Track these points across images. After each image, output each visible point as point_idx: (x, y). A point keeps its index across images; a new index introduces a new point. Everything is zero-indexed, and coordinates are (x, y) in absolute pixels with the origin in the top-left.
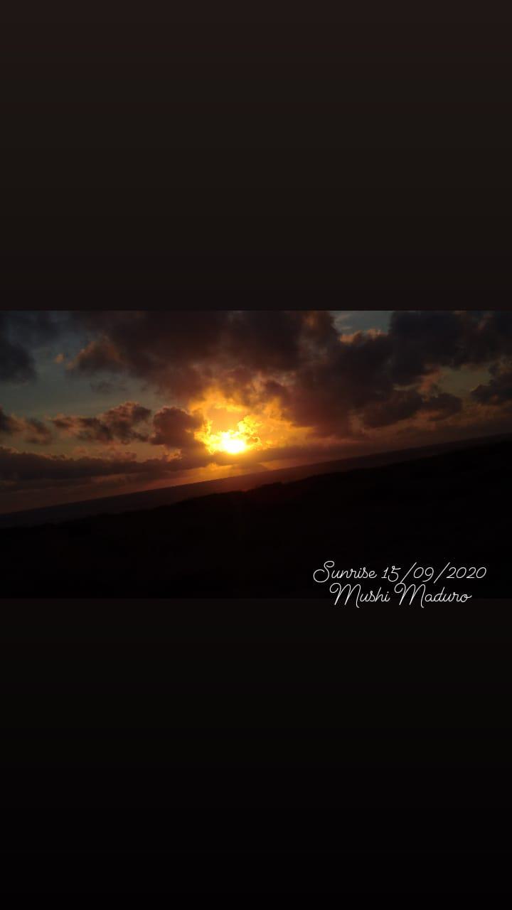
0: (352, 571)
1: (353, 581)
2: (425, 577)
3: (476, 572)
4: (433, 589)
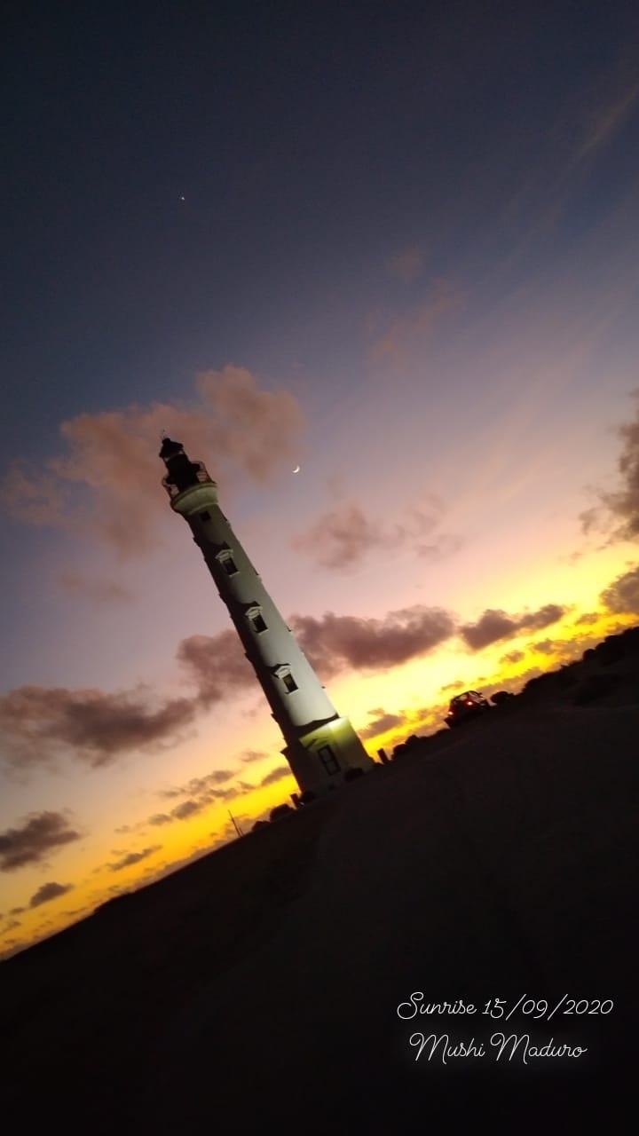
0: (445, 1004)
2: (536, 1013)
3: (600, 1006)
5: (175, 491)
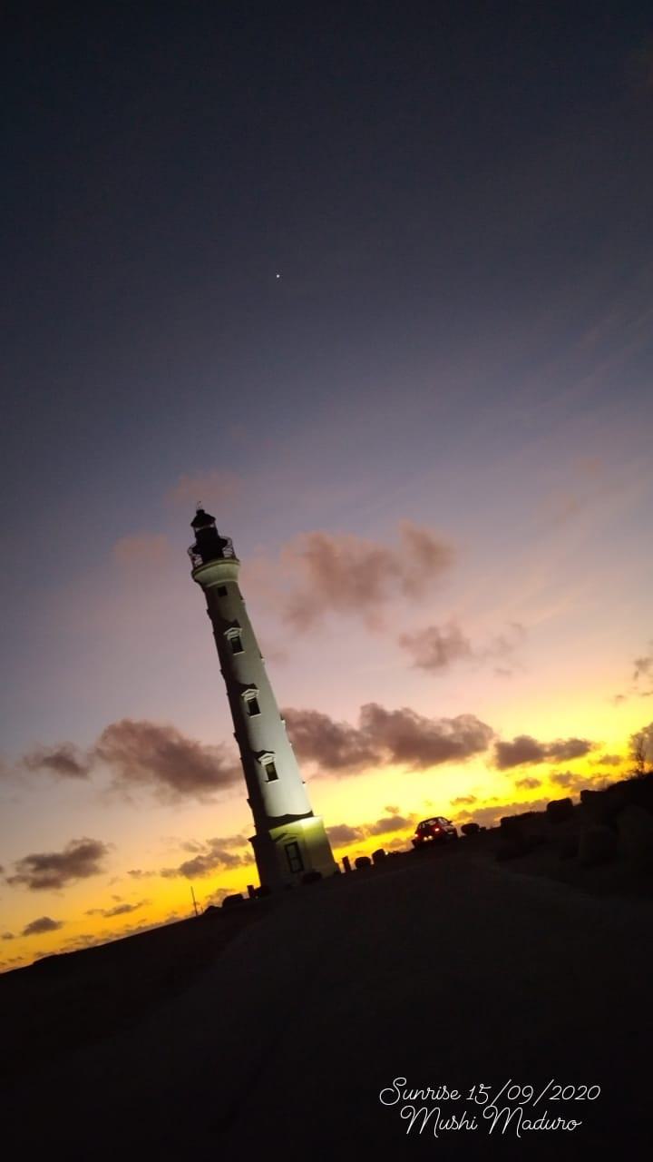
0: (429, 1090)
1: (430, 1104)
2: (521, 1098)
3: (587, 1091)
4: (532, 1113)
5: (199, 561)
